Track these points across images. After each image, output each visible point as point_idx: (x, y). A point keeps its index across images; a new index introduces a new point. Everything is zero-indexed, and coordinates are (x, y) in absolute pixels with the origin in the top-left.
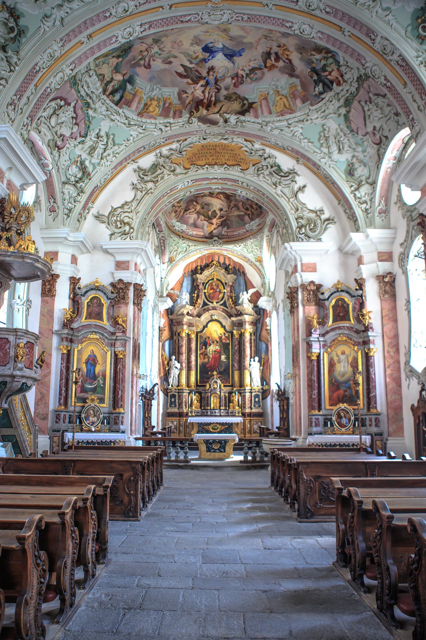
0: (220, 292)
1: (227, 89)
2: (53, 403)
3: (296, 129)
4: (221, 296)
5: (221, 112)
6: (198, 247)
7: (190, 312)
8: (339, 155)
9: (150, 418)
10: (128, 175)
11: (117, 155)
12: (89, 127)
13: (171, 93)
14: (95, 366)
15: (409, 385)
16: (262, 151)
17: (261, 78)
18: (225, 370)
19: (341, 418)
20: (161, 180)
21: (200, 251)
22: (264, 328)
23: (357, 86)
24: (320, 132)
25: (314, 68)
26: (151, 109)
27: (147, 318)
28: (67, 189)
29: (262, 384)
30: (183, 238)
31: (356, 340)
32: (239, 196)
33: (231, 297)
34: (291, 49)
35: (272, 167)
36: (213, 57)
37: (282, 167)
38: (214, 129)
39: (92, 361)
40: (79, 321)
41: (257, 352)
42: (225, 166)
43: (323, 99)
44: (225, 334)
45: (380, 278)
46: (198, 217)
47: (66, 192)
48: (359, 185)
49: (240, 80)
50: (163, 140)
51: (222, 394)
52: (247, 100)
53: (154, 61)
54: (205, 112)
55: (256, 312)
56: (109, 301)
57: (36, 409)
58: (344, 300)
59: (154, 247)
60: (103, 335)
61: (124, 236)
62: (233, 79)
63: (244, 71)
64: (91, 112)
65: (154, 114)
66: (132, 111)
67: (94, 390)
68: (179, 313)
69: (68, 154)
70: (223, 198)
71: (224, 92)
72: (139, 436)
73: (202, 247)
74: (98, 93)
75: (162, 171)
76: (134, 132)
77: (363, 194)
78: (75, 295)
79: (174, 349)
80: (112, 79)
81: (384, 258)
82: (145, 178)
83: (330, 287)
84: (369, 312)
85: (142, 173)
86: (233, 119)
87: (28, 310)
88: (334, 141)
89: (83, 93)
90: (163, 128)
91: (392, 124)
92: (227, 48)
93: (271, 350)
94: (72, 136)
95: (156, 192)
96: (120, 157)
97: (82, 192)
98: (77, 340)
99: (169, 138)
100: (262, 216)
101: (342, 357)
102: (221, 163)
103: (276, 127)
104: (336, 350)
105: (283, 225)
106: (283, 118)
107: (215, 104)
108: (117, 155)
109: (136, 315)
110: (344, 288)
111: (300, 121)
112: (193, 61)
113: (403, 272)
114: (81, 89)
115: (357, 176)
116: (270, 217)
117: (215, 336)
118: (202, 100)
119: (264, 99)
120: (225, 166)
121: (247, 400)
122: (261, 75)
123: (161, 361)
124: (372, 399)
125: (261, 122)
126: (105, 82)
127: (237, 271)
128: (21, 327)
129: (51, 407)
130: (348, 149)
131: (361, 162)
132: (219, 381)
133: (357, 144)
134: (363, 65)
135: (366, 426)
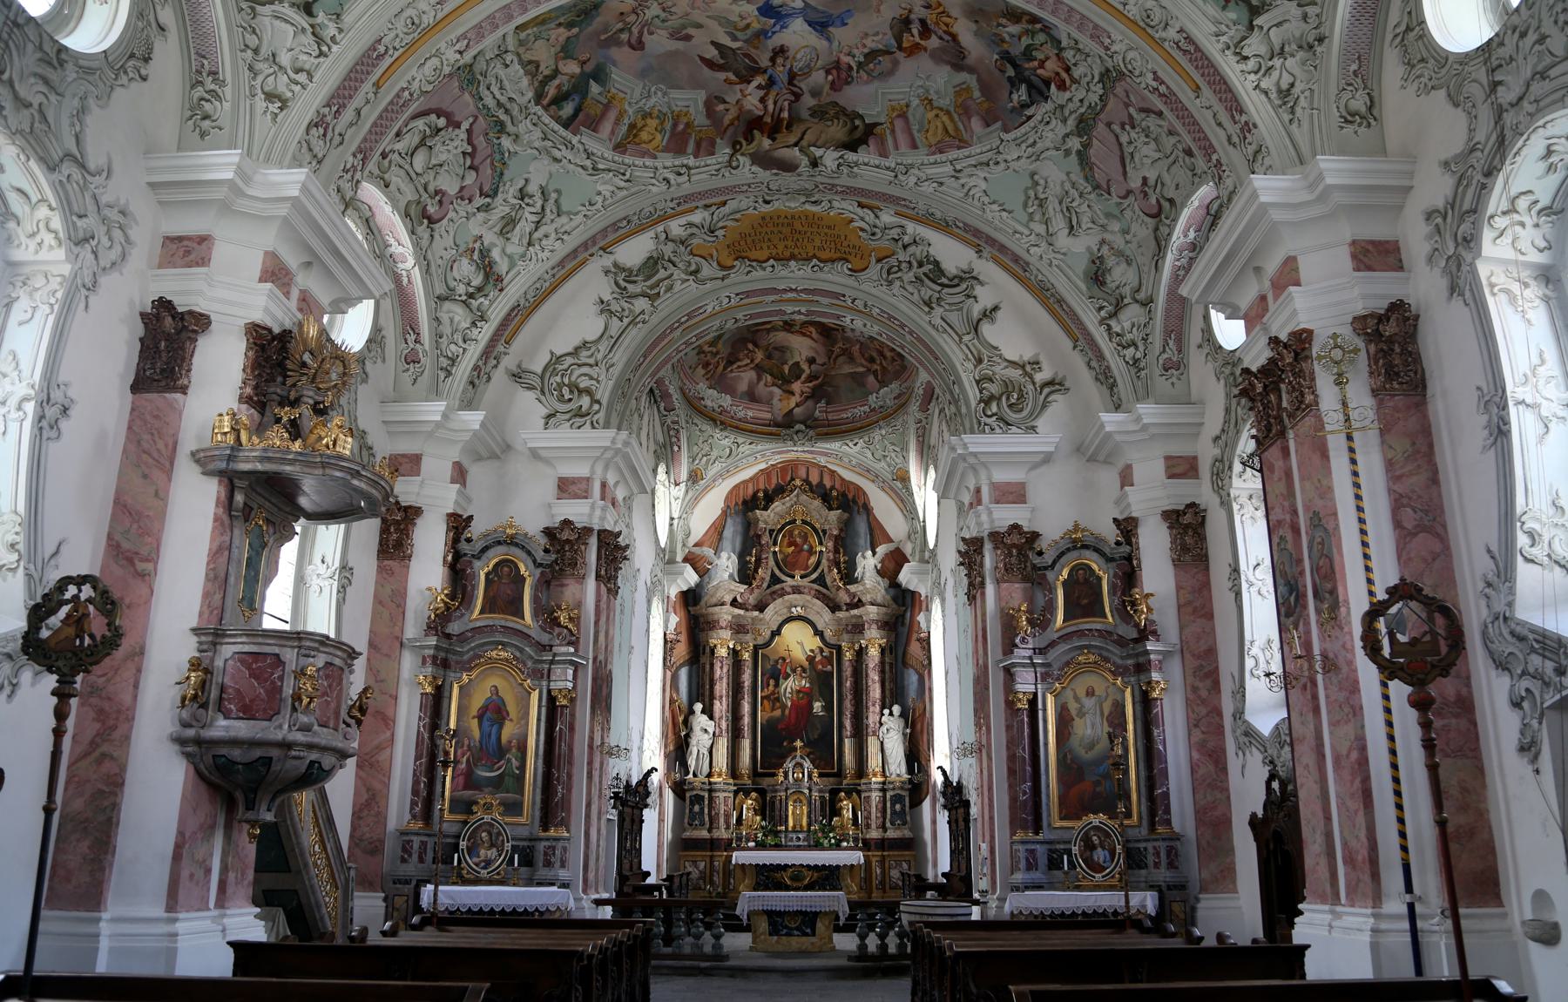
0: (811, 552)
1: (815, 93)
2: (398, 809)
4: (813, 560)
5: (804, 143)
8: (1071, 240)
10: (593, 283)
13: (690, 101)
16: (899, 230)
17: (891, 73)
19: (1093, 848)
22: (915, 636)
24: (1027, 189)
26: (644, 136)
27: (633, 612)
28: (449, 312)
29: (910, 770)
30: (724, 426)
31: (1119, 662)
34: (955, 12)
35: (920, 265)
37: (944, 266)
39: (495, 712)
40: (466, 618)
41: (894, 693)
42: (815, 261)
43: (1029, 118)
44: (822, 651)
45: (1172, 517)
46: (759, 378)
47: (445, 318)
48: (1119, 306)
49: (844, 75)
52: (861, 117)
53: (651, 33)
54: (767, 143)
55: (895, 599)
56: (538, 572)
57: (354, 828)
60: (521, 651)
62: (828, 72)
64: (506, 142)
65: (650, 147)
66: (601, 140)
67: (497, 784)
68: (714, 600)
70: (814, 335)
71: (808, 101)
72: (605, 896)
73: (768, 446)
74: (523, 100)
76: (605, 185)
77: (1127, 325)
78: (458, 555)
80: (556, 72)
82: (631, 287)
85: (623, 276)
86: (830, 158)
87: (342, 590)
88: (1058, 208)
90: (671, 177)
91: (1181, 174)
93: (931, 690)
96: (572, 242)
97: (482, 318)
98: (457, 663)
99: (687, 198)
100: (905, 375)
101: (1089, 703)
103: (926, 175)
104: (1073, 685)
105: (948, 396)
106: (943, 157)
107: (789, 127)
109: (603, 605)
110: (1090, 541)
112: (738, 34)
115: (1113, 285)
116: (923, 376)
117: (799, 655)
118: (761, 117)
120: (815, 261)
123: (667, 713)
124: (1159, 801)
127: (848, 502)
128: (325, 632)
129: (393, 823)
131: (1120, 254)
132: (807, 764)
133: (1108, 215)
134: (1107, 49)
135: (1146, 866)
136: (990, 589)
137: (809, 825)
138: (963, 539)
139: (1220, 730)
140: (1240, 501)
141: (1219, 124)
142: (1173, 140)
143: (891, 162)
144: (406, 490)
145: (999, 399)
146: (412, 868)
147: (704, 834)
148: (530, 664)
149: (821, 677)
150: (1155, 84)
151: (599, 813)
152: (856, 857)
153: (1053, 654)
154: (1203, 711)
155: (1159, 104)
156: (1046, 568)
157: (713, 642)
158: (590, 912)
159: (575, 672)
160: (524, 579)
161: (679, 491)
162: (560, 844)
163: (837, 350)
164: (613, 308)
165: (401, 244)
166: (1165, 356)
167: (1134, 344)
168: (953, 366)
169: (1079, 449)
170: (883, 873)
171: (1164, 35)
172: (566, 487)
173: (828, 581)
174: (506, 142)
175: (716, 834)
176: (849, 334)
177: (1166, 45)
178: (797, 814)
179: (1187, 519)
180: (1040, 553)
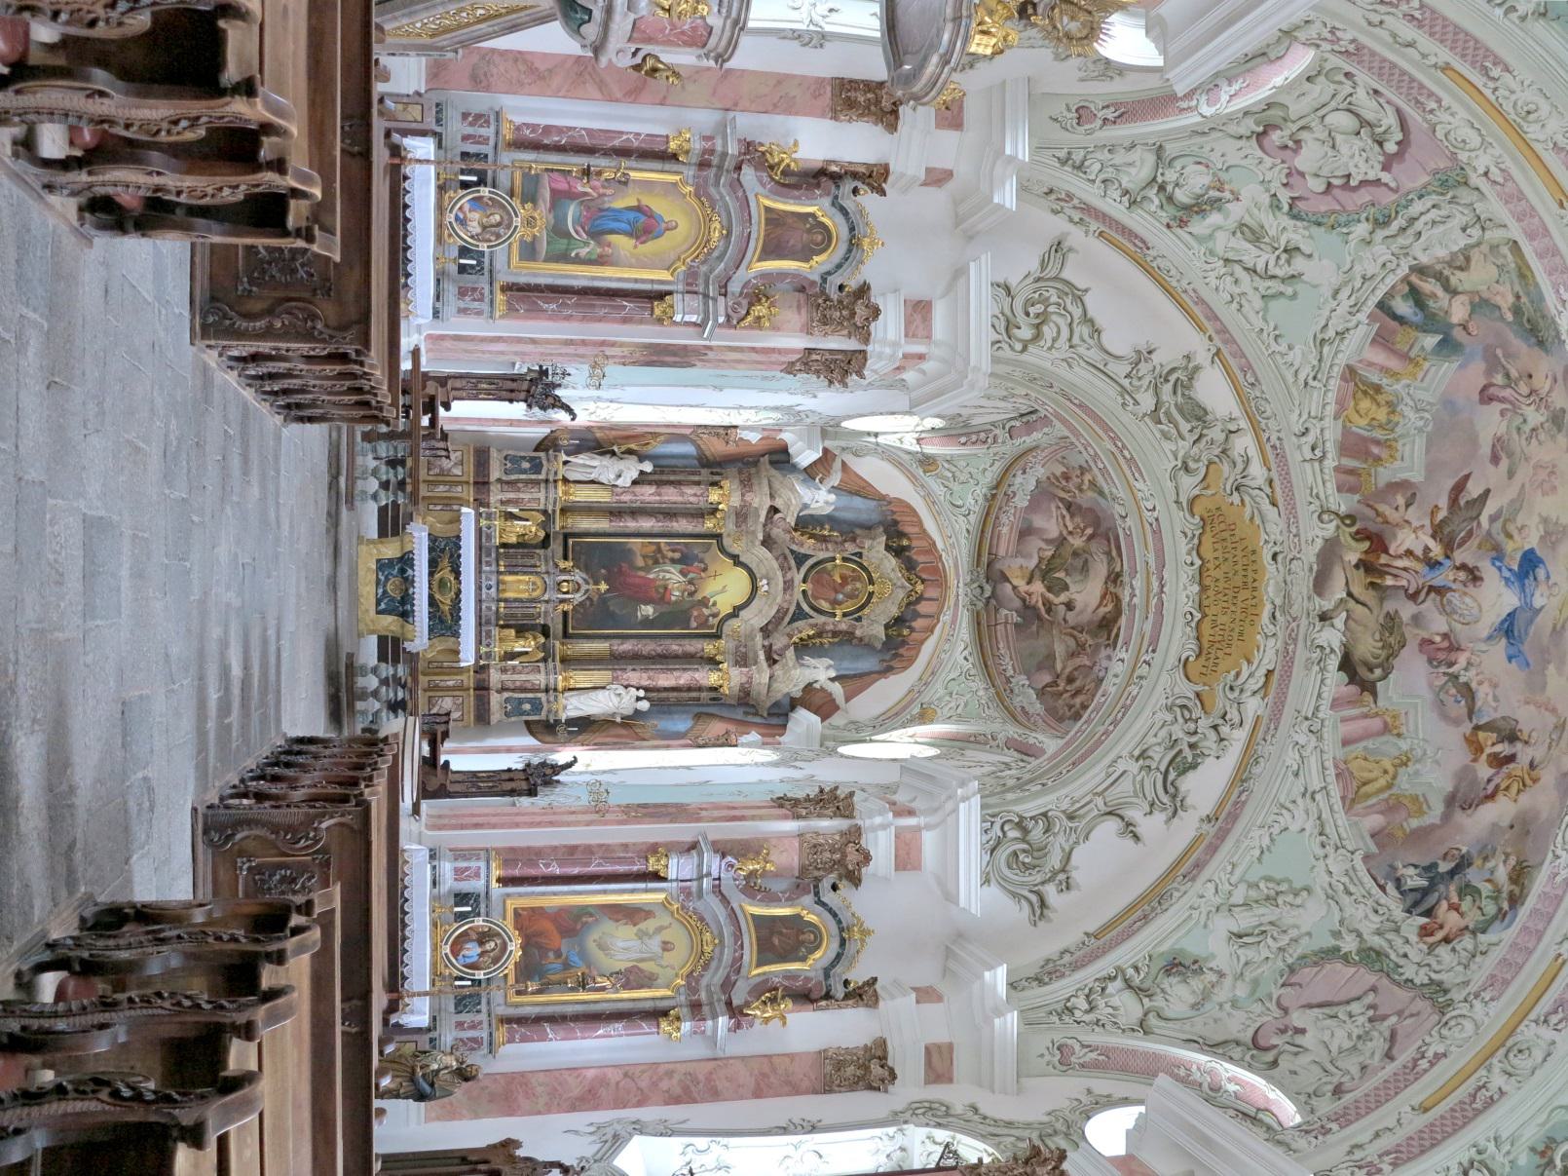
0: (835, 603)
1: (1416, 619)
3: (1299, 813)
4: (825, 605)
5: (1352, 604)
6: (963, 541)
8: (1226, 934)
9: (476, 398)
10: (1178, 339)
11: (1235, 305)
12: (1319, 224)
13: (1410, 462)
14: (630, 234)
15: (576, 1132)
16: (1237, 720)
17: (1445, 717)
18: (612, 615)
19: (481, 943)
20: (1162, 432)
21: (953, 546)
22: (732, 728)
23: (1417, 981)
24: (1290, 881)
25: (1470, 865)
26: (1365, 404)
27: (763, 390)
28: (1143, 161)
29: (571, 722)
31: (704, 982)
32: (1109, 658)
33: (819, 635)
35: (1192, 746)
36: (1507, 580)
37: (1191, 775)
38: (1303, 583)
39: (644, 226)
40: (760, 189)
41: (663, 701)
42: (1198, 616)
43: (1382, 888)
44: (715, 616)
46: (1048, 542)
47: (1135, 155)
49: (1441, 656)
50: (1274, 438)
51: (543, 607)
53: (1502, 413)
54: (1353, 557)
55: (776, 704)
56: (817, 278)
57: (503, 53)
58: (818, 947)
59: (965, 412)
61: (1003, 324)
62: (1445, 636)
63: (1466, 669)
64: (1362, 229)
65: (1351, 412)
66: (1360, 350)
67: (558, 231)
68: (776, 485)
69: (1243, 163)
70: (1103, 610)
71: (1406, 610)
72: (423, 360)
73: (965, 551)
75: (1187, 435)
76: (1302, 355)
77: (1115, 1001)
78: (836, 178)
79: (673, 469)
80: (1454, 292)
81: (935, 1058)
82: (1169, 387)
83: (854, 909)
84: (783, 1018)
85: (1183, 378)
86: (1332, 637)
87: (796, 36)
88: (1265, 920)
89: (1417, 207)
90: (1310, 439)
91: (1310, 1078)
92: (1531, 621)
93: (668, 747)
94: (1294, 174)
95: (1126, 418)
96: (1228, 314)
97: (1133, 203)
98: (706, 180)
99: (1281, 457)
102: (1205, 603)
105: (1027, 776)
108: (1235, 305)
109: (775, 357)
111: (1322, 825)
112: (1498, 524)
113: (896, 1113)
114: (1428, 201)
115: (1165, 985)
116: (1051, 744)
118: (1386, 551)
119: (1386, 724)
120: (1198, 616)
121: (523, 677)
122: (1453, 714)
123: (640, 430)
125: (1321, 715)
126: (1446, 272)
130: (1243, 960)
131: (1206, 995)
132: (578, 597)
133: (1256, 983)
136: (791, 826)
138: (852, 794)
139: (620, 1103)
140: (899, 1136)
141: (1377, 1135)
142: (1355, 1070)
143: (1325, 712)
144: (916, 119)
145: (1023, 840)
146: (455, 128)
147: (495, 473)
148: (704, 268)
149: (676, 616)
150: (1430, 1054)
151: (524, 354)
152: (468, 658)
153: (714, 902)
154: (644, 1084)
155: (1404, 1057)
156: (817, 894)
157: (726, 484)
158: (406, 343)
159: (695, 324)
160: (807, 260)
161: (910, 444)
162: (485, 307)
163: (1083, 637)
164: (1142, 365)
165: (1231, 101)
166: (1077, 1047)
167: (1091, 1009)
168: (1064, 784)
169: (960, 936)
170: (449, 689)
171: (1496, 1070)
172: (919, 311)
174: (1362, 229)
175: (494, 488)
176: (1104, 653)
177: (1483, 1072)
178: (519, 586)
179: (876, 1069)
180: (834, 888)
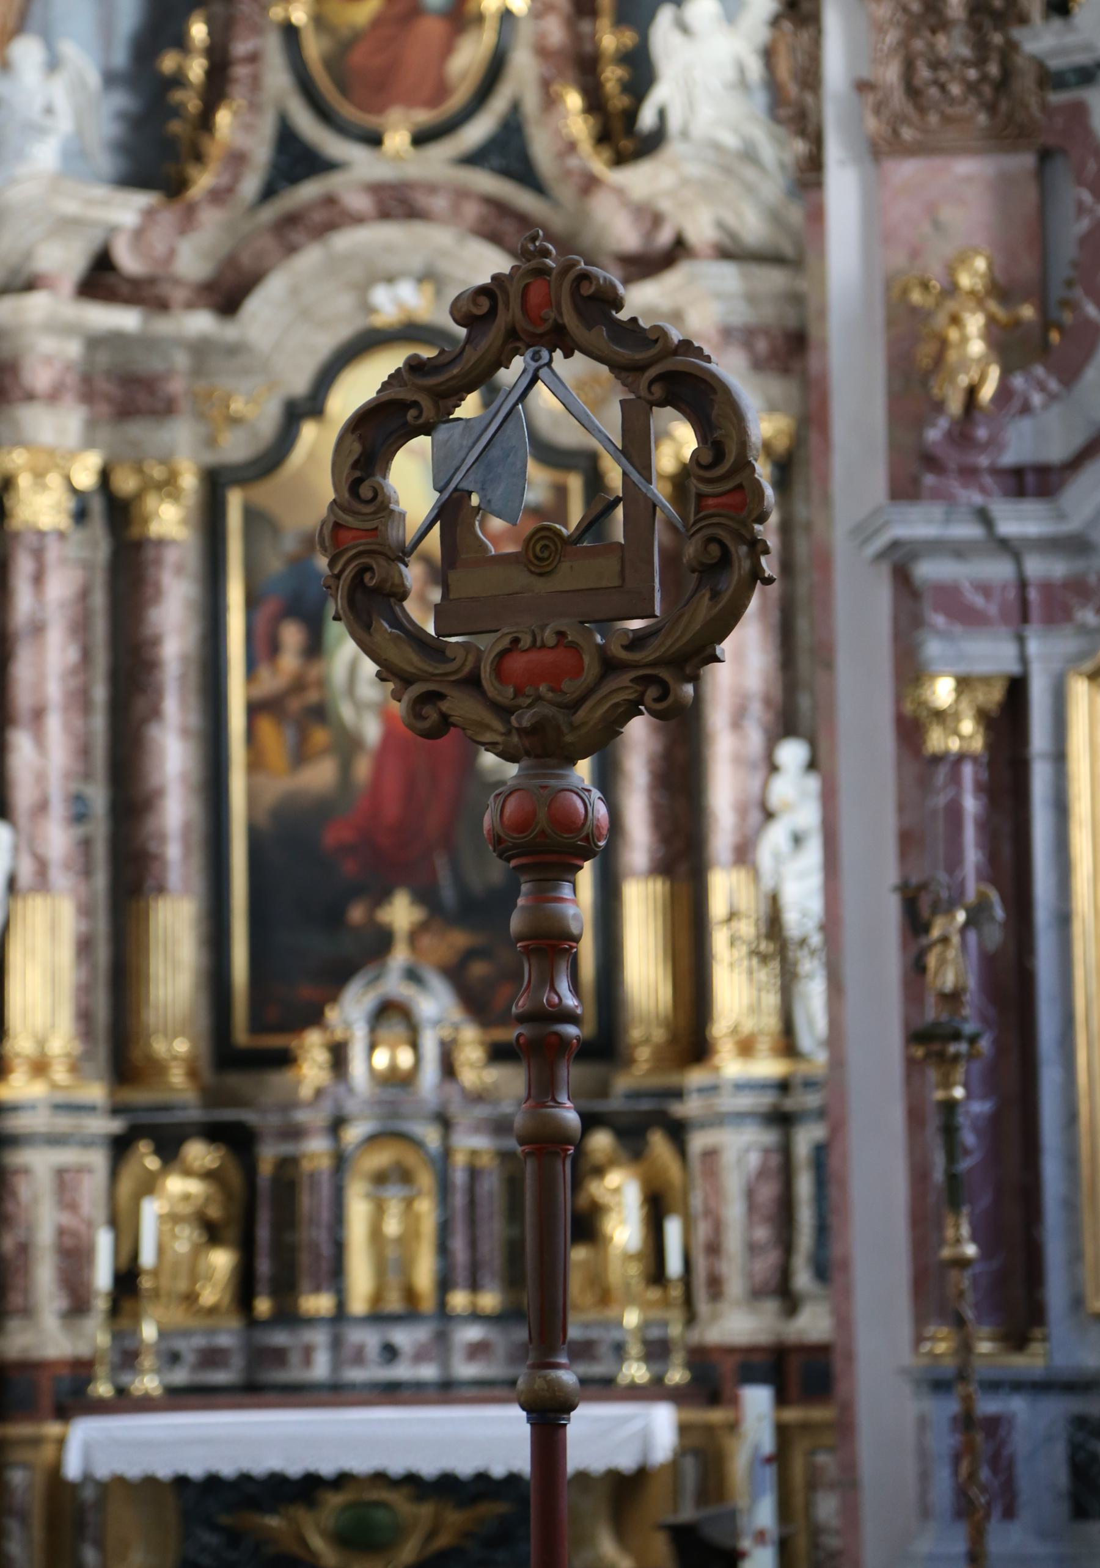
4: (469, 56)
7: (128, 261)
137: (444, 1284)
173: (542, 149)
